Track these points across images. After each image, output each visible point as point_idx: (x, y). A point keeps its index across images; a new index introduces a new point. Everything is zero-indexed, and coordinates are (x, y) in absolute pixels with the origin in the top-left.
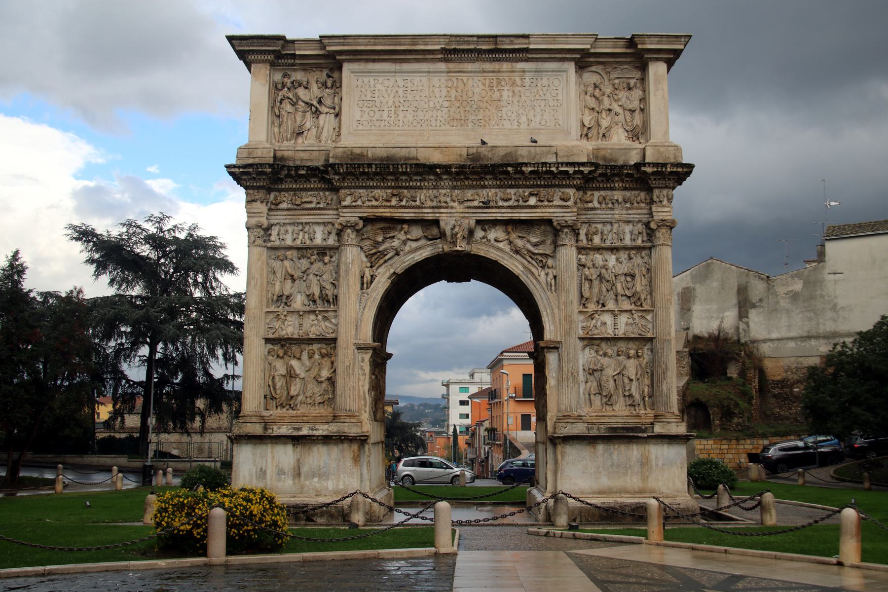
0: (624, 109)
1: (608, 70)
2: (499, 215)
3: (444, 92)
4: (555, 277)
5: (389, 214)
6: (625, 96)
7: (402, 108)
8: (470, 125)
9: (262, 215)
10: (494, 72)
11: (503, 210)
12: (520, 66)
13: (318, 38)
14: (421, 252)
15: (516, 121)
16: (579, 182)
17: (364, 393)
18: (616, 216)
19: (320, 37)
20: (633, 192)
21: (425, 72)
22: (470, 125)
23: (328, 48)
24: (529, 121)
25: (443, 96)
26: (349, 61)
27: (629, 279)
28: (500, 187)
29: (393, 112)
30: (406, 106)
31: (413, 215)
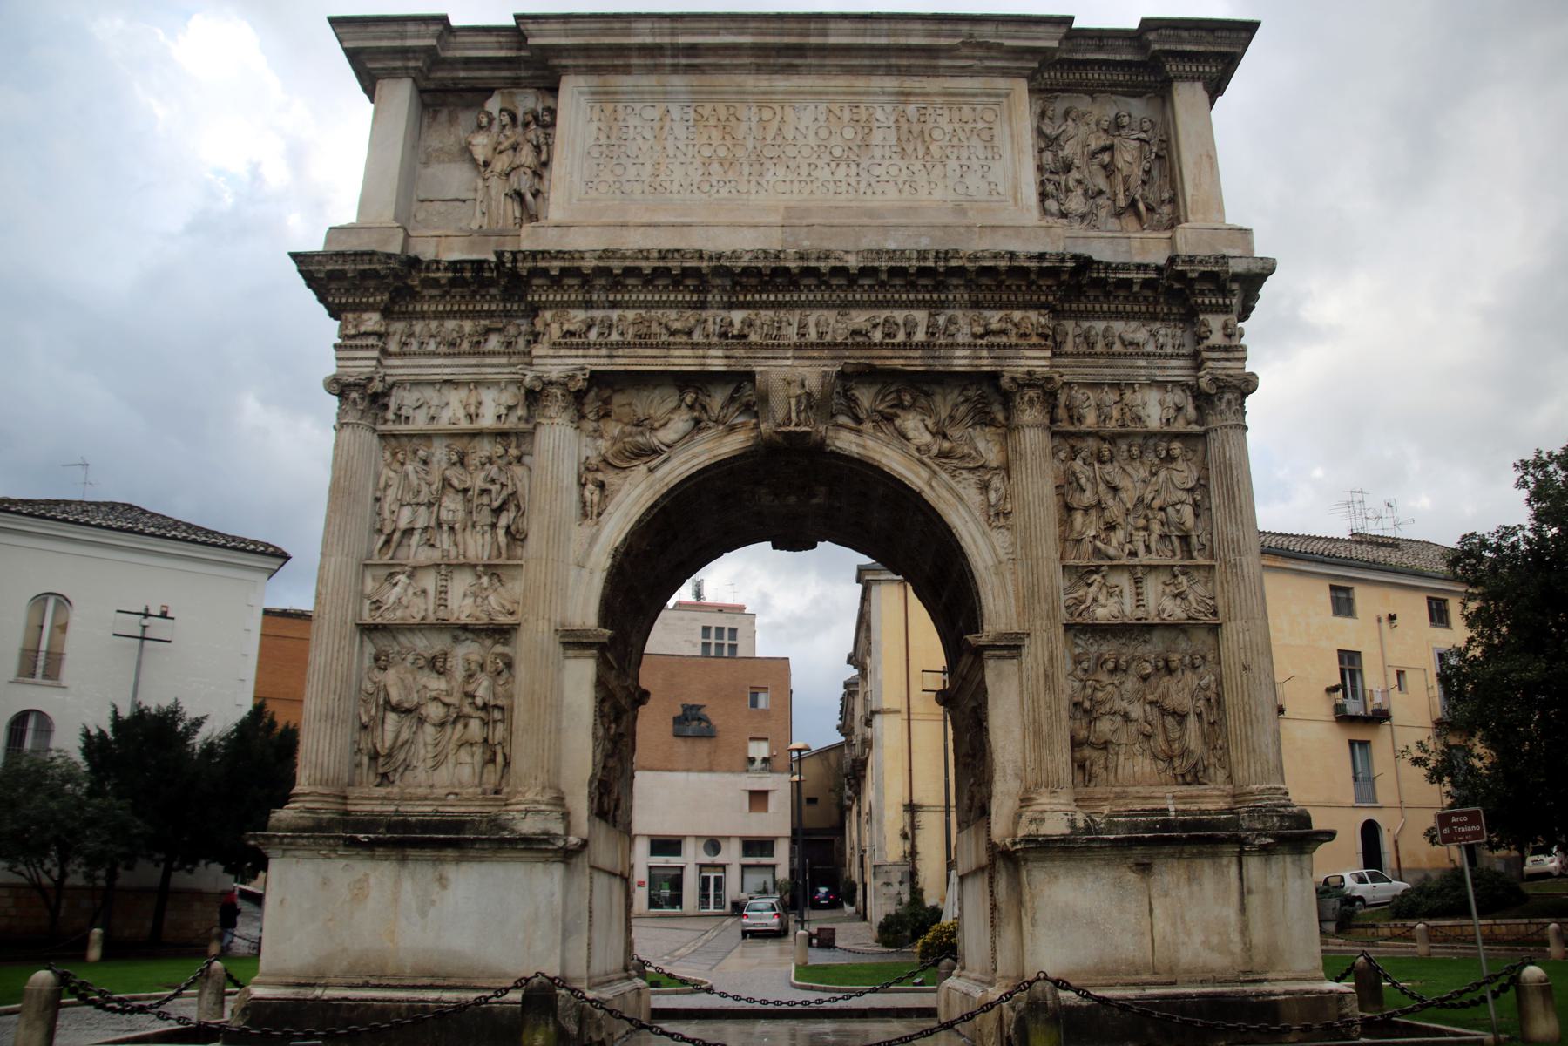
7: (682, 159)
13: (512, 23)
19: (517, 17)
23: (531, 41)
26: (577, 70)
30: (690, 155)
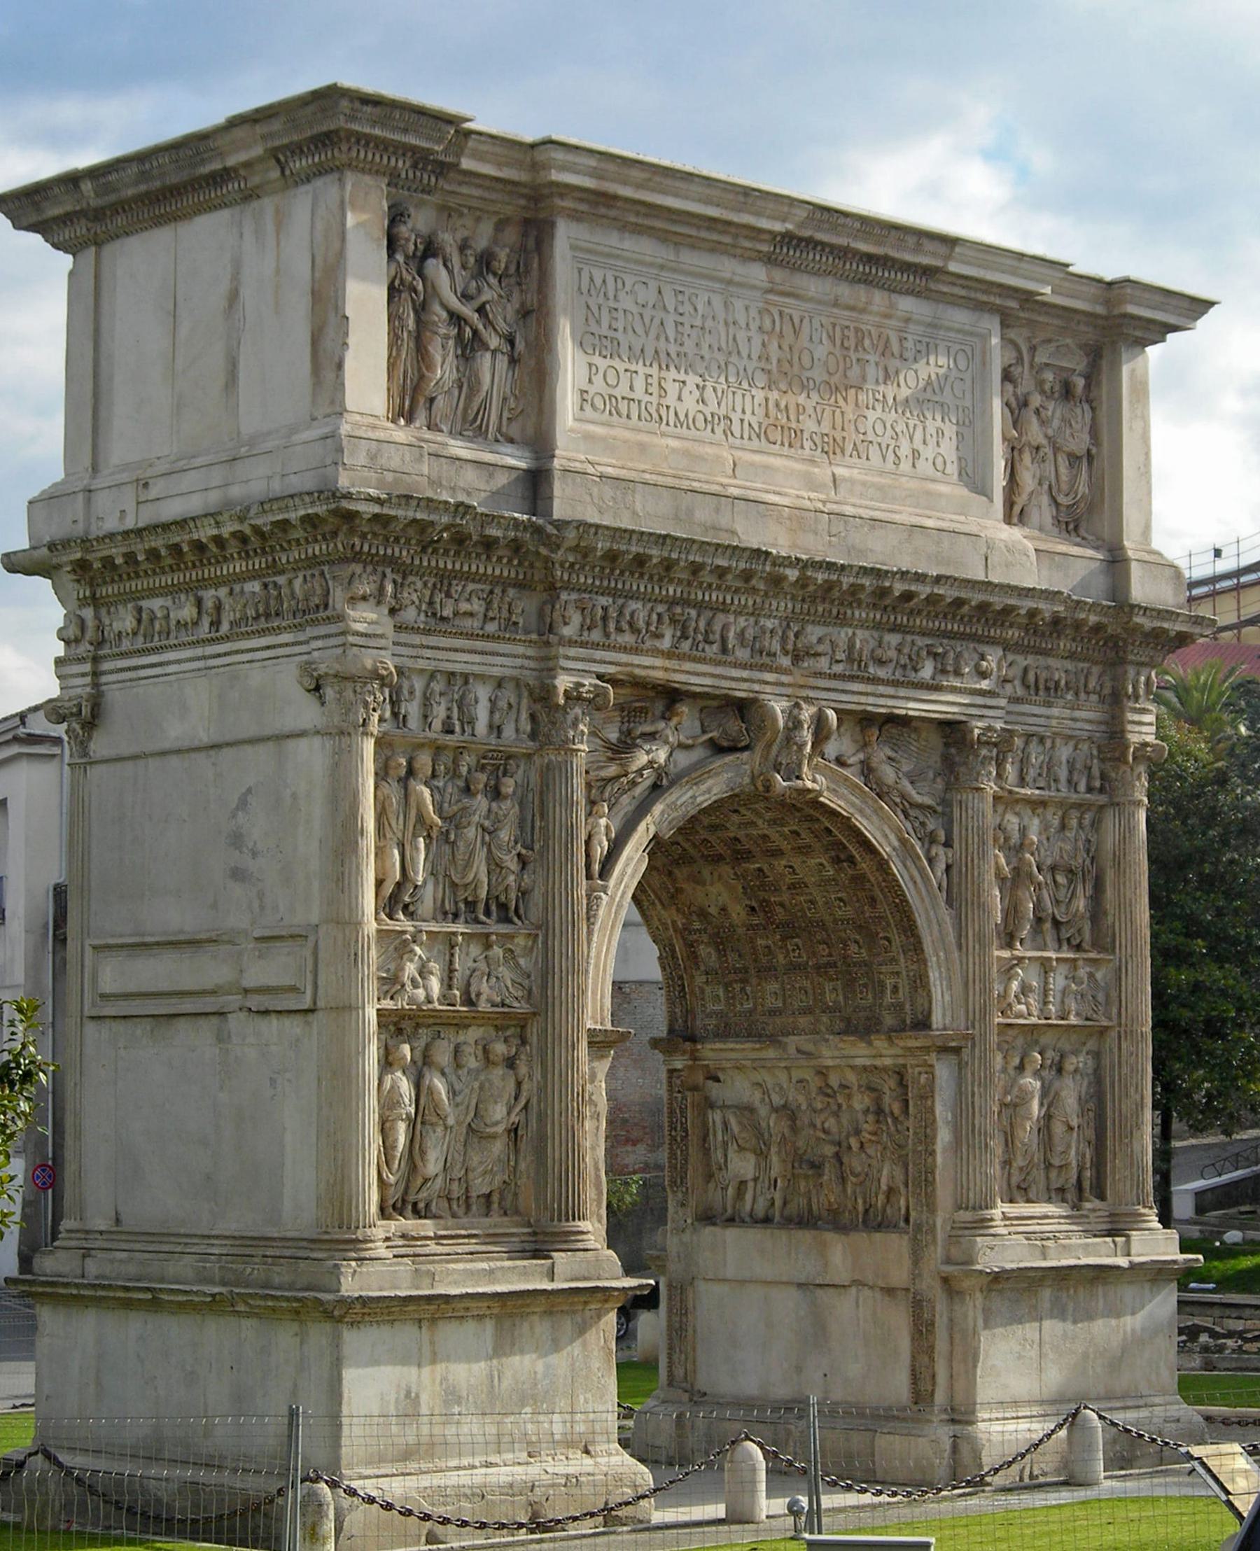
0: (1056, 450)
1: (1035, 342)
2: (871, 700)
3: (757, 342)
4: (948, 868)
5: (659, 675)
6: (1058, 414)
8: (807, 444)
9: (382, 643)
10: (853, 309)
11: (881, 689)
12: (906, 304)
14: (710, 782)
15: (891, 448)
16: (1017, 635)
17: (597, 1169)
18: (1054, 722)
20: (1081, 665)
21: (721, 280)
22: (807, 444)
24: (916, 454)
25: (755, 356)
27: (1061, 879)
28: (877, 626)
29: (654, 381)
31: (708, 681)
